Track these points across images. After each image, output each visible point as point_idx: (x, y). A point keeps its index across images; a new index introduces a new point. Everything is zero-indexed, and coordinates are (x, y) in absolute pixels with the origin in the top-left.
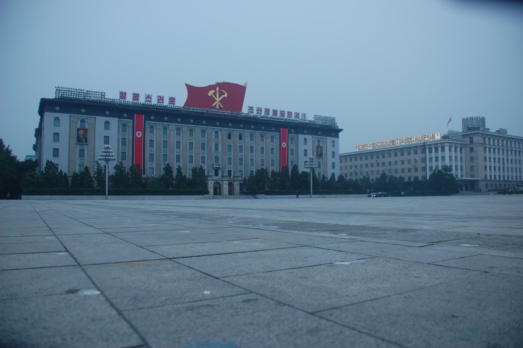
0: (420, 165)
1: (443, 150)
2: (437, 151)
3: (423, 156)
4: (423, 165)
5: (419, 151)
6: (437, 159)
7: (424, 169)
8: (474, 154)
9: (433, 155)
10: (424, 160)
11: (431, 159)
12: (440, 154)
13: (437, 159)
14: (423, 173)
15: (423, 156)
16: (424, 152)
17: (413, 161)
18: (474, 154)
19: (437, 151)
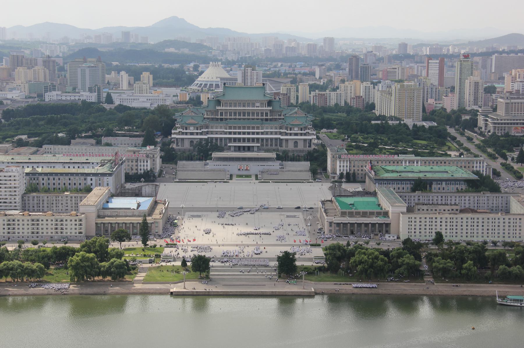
0: (134, 168)
1: (147, 162)
2: (144, 162)
3: (137, 164)
4: (137, 168)
5: (134, 161)
6: (144, 166)
7: (137, 169)
8: (155, 162)
9: (142, 164)
10: (137, 166)
11: (141, 166)
12: (145, 164)
13: (144, 166)
14: (136, 171)
15: (137, 164)
16: (137, 161)
17: (130, 166)
18: (155, 162)
19: (144, 162)
